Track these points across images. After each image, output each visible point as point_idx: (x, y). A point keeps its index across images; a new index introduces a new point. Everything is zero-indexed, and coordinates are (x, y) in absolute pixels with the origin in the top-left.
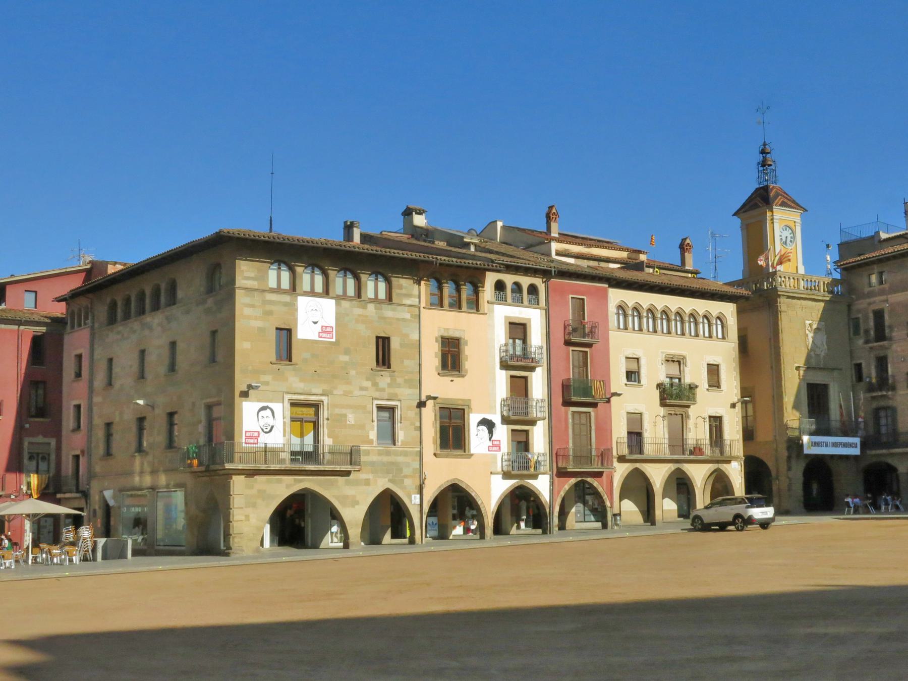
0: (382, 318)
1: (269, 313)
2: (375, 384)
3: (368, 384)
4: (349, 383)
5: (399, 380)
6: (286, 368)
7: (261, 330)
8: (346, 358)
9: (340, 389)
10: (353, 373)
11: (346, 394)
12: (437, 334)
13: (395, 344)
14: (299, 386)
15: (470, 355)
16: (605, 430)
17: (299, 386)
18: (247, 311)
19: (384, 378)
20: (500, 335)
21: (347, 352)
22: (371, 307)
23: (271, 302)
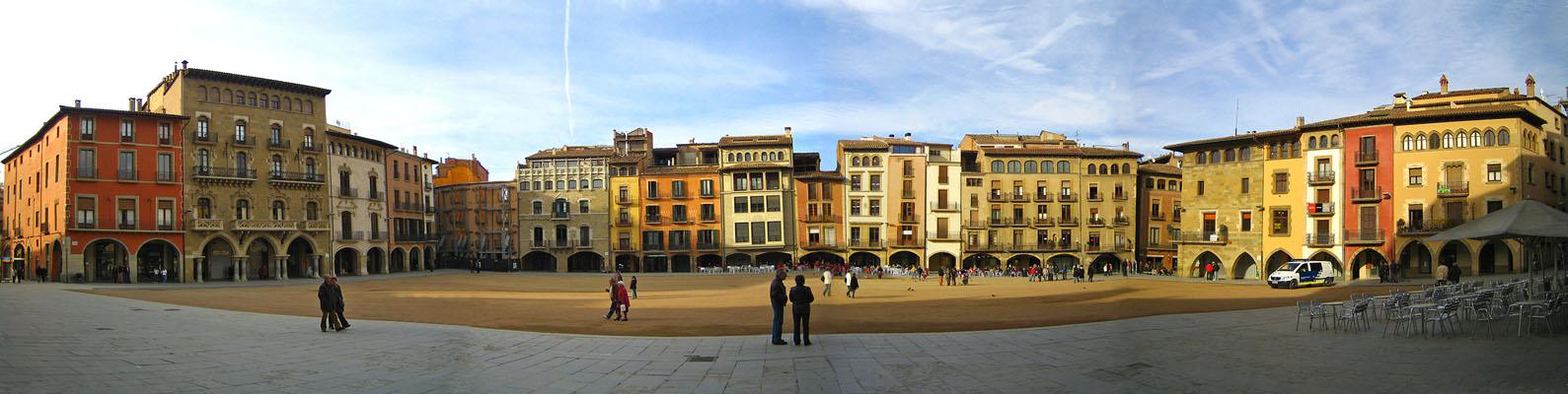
0: (1245, 170)
1: (1194, 176)
2: (1240, 202)
3: (1237, 202)
4: (1228, 202)
5: (1253, 199)
6: (1201, 199)
7: (1192, 183)
8: (1227, 191)
9: (1224, 205)
10: (1230, 197)
11: (1227, 208)
12: (1272, 172)
13: (1251, 181)
14: (1207, 206)
15: (1293, 182)
16: (1388, 216)
17: (1207, 206)
18: (1187, 177)
19: (1245, 199)
20: (1311, 167)
21: (1227, 188)
22: (1239, 165)
23: (1196, 171)
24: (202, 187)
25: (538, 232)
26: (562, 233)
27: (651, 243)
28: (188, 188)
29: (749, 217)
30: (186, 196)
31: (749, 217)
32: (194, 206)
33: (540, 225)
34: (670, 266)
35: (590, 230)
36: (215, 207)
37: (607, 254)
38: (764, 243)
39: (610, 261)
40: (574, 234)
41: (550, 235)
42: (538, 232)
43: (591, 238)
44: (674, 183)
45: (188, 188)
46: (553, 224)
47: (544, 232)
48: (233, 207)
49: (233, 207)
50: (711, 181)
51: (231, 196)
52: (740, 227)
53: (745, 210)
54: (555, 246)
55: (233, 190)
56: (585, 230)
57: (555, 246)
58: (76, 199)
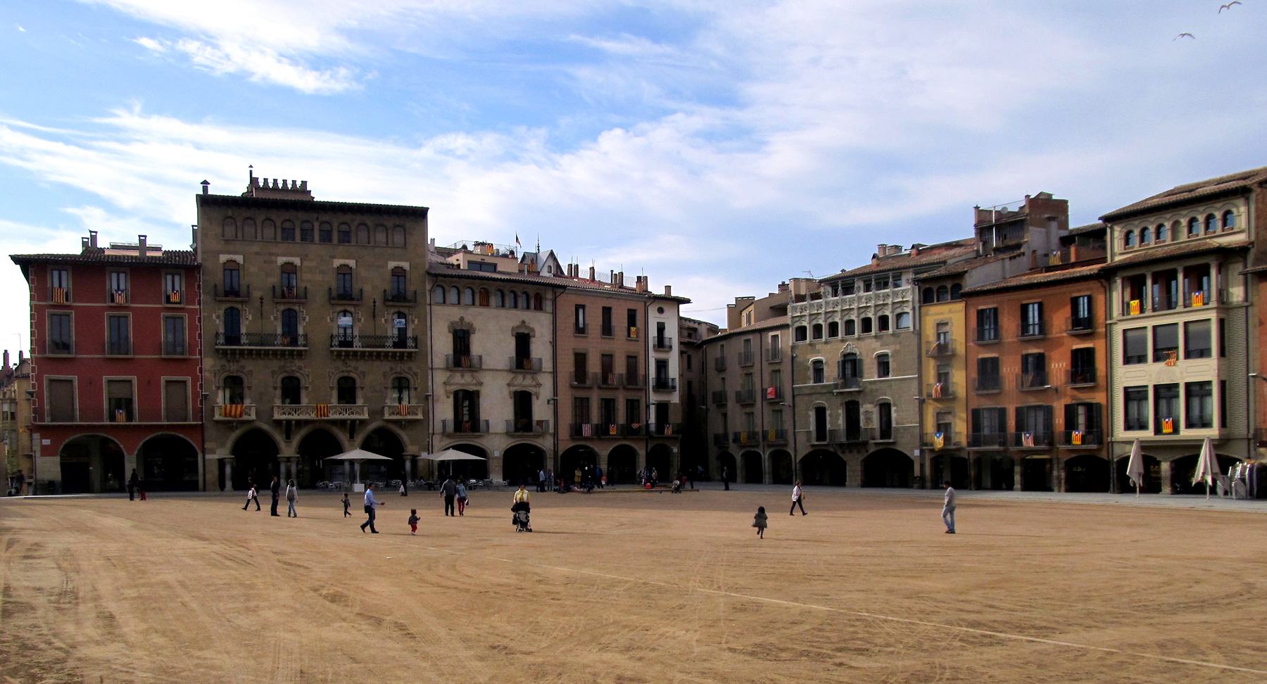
24: (229, 361)
25: (821, 413)
26: (852, 410)
27: (986, 432)
28: (208, 363)
29: (1149, 374)
30: (206, 374)
31: (1149, 374)
32: (218, 388)
33: (821, 401)
34: (1017, 478)
35: (893, 409)
36: (249, 388)
37: (917, 453)
38: (1176, 430)
39: (922, 466)
40: (869, 416)
41: (837, 420)
42: (821, 413)
43: (894, 425)
44: (1129, 314)
45: (208, 363)
46: (839, 400)
47: (828, 412)
48: (275, 388)
49: (275, 388)
50: (1090, 298)
51: (273, 373)
52: (1134, 395)
53: (1141, 359)
54: (843, 440)
55: (275, 364)
56: (885, 408)
57: (843, 440)
58: (45, 383)
